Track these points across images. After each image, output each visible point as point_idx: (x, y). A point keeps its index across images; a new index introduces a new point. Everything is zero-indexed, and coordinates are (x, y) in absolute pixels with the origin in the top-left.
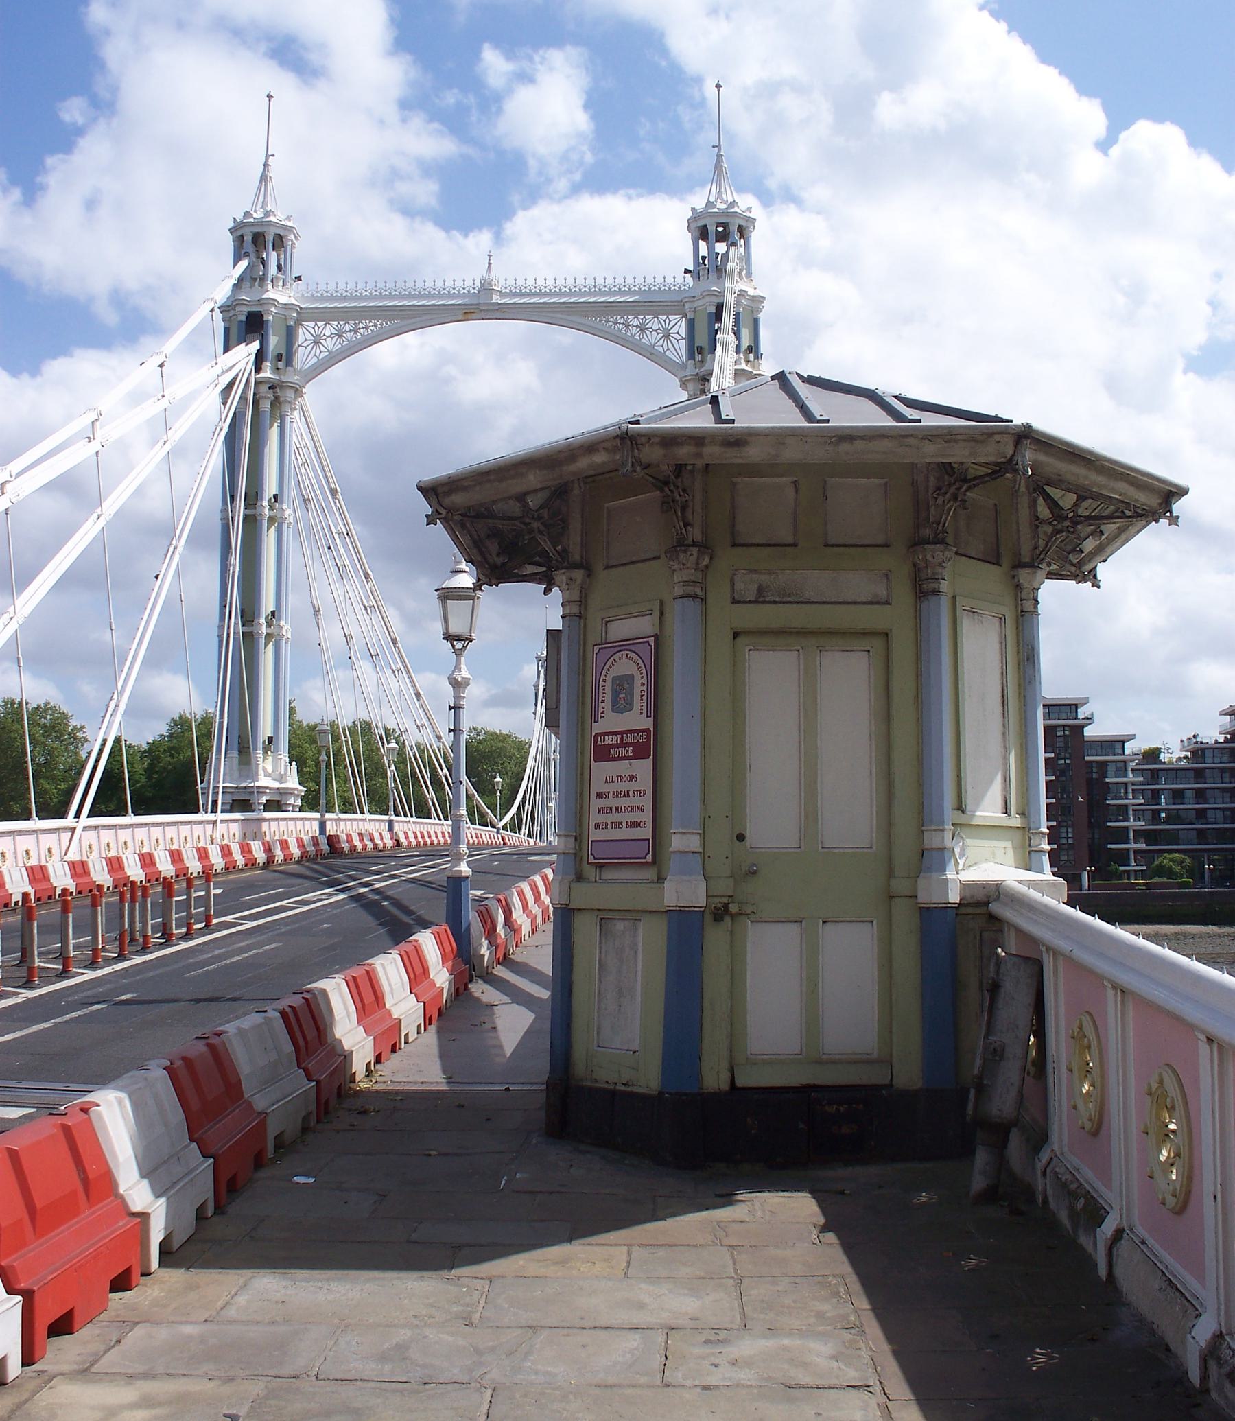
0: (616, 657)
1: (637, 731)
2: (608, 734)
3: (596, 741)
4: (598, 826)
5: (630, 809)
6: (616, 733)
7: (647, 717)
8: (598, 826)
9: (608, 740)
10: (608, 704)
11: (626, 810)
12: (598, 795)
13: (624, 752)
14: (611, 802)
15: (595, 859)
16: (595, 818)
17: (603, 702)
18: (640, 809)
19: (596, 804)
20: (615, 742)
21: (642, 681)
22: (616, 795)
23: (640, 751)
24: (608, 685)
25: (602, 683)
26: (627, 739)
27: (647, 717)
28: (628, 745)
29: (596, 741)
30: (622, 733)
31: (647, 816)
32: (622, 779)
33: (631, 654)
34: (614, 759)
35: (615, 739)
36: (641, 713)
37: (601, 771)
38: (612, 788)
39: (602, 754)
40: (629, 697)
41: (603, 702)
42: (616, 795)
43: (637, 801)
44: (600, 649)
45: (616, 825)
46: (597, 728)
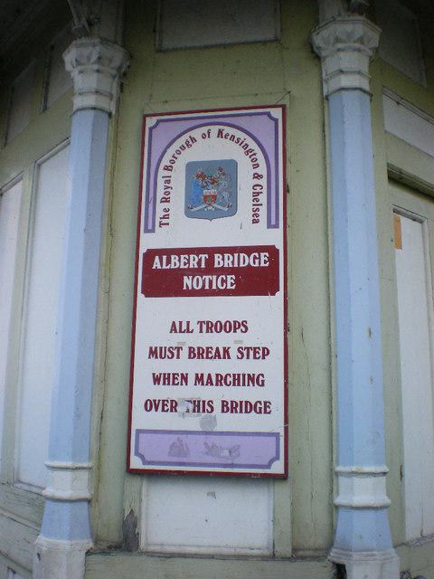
0: (197, 133)
1: (248, 250)
2: (179, 252)
4: (151, 405)
5: (230, 379)
6: (198, 251)
7: (269, 226)
8: (151, 405)
9: (176, 262)
11: (221, 380)
13: (217, 283)
14: (183, 365)
15: (145, 462)
16: (145, 389)
17: (166, 200)
18: (255, 380)
19: (146, 367)
20: (193, 264)
21: (257, 170)
22: (196, 353)
25: (162, 173)
27: (269, 226)
30: (211, 252)
31: (272, 391)
32: (211, 327)
33: (227, 130)
36: (255, 221)
37: (157, 314)
39: (162, 282)
40: (226, 194)
41: (166, 200)
42: (196, 353)
43: (249, 366)
45: (199, 406)
46: (148, 242)
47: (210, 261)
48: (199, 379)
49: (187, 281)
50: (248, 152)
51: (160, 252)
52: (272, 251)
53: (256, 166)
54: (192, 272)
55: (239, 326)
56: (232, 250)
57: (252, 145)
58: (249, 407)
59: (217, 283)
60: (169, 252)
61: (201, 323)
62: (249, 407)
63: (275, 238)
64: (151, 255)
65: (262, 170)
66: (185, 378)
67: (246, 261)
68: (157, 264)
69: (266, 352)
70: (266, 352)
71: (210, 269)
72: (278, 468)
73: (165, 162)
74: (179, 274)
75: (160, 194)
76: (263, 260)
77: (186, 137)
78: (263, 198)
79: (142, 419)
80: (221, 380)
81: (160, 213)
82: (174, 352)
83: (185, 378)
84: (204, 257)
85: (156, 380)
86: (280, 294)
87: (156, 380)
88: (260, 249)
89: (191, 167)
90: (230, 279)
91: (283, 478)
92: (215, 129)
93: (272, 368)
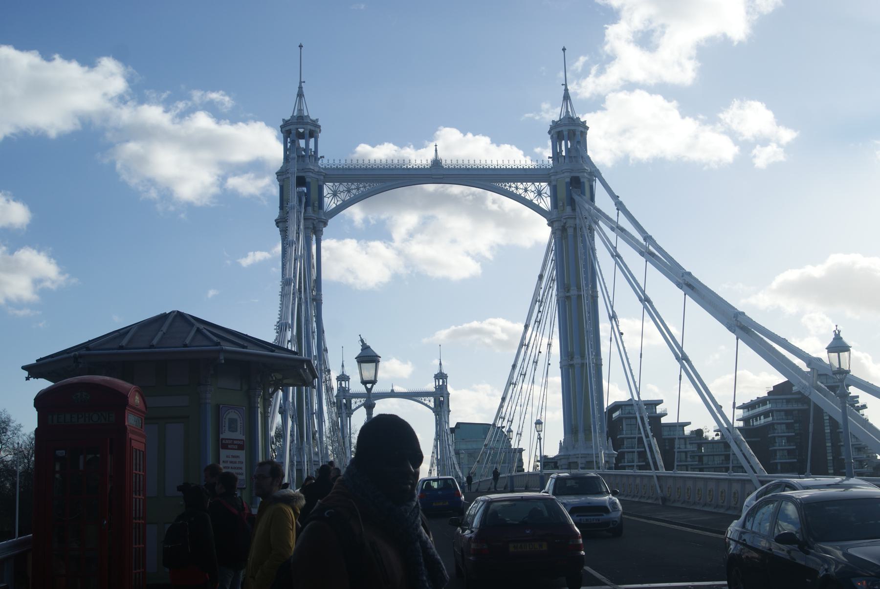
0: (230, 411)
1: (240, 440)
2: (227, 439)
3: (222, 441)
7: (243, 435)
9: (227, 442)
10: (227, 428)
11: (235, 468)
12: (223, 462)
17: (224, 427)
18: (241, 468)
20: (230, 442)
22: (231, 462)
23: (241, 447)
24: (227, 421)
25: (224, 420)
26: (235, 442)
27: (243, 435)
28: (235, 444)
29: (222, 441)
30: (233, 440)
32: (233, 457)
33: (236, 411)
35: (230, 442)
39: (225, 447)
41: (224, 427)
42: (231, 462)
43: (240, 465)
44: (223, 407)
46: (222, 436)
47: (233, 442)
49: (229, 446)
50: (240, 417)
52: (243, 440)
53: (241, 421)
55: (238, 457)
61: (232, 456)
63: (243, 438)
64: (222, 439)
65: (242, 422)
66: (229, 467)
67: (239, 442)
68: (223, 442)
70: (242, 463)
71: (233, 444)
72: (245, 486)
73: (224, 417)
74: (228, 444)
75: (223, 426)
76: (241, 443)
77: (227, 412)
80: (235, 468)
81: (224, 430)
83: (229, 467)
84: (232, 441)
86: (245, 451)
88: (241, 440)
89: (230, 419)
90: (237, 446)
91: (244, 488)
93: (244, 466)
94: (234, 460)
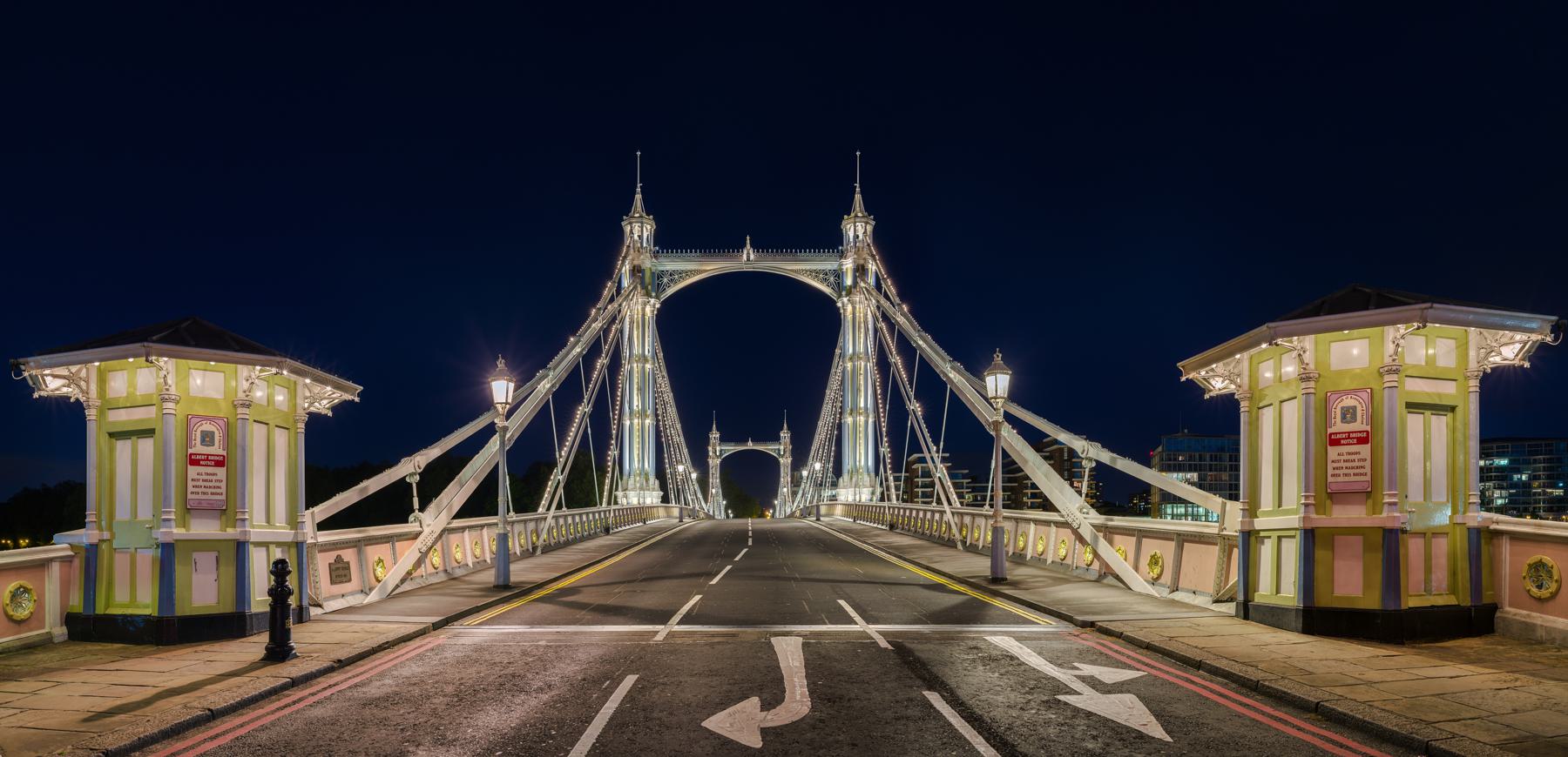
0: (1344, 398)
2: (1339, 433)
6: (1345, 433)
8: (1333, 475)
9: (1339, 436)
11: (1353, 468)
14: (1342, 464)
16: (1330, 471)
24: (1339, 411)
26: (1351, 435)
28: (1354, 438)
32: (1349, 454)
33: (1353, 396)
34: (1344, 445)
38: (1342, 458)
48: (1346, 468)
49: (1342, 442)
50: (1360, 403)
51: (1334, 434)
52: (1367, 432)
54: (1343, 439)
56: (1355, 432)
57: (1361, 401)
58: (1361, 474)
59: (1351, 442)
60: (1336, 433)
62: (1361, 474)
63: (1369, 428)
64: (1331, 434)
65: (1364, 408)
67: (1359, 435)
69: (1366, 460)
70: (1366, 460)
75: (1333, 416)
78: (1365, 417)
79: (1330, 479)
80: (1353, 468)
82: (1339, 461)
85: (1334, 469)
87: (1334, 469)
88: (1364, 432)
89: (1342, 408)
91: (1371, 492)
92: (1349, 396)
94: (1353, 457)
